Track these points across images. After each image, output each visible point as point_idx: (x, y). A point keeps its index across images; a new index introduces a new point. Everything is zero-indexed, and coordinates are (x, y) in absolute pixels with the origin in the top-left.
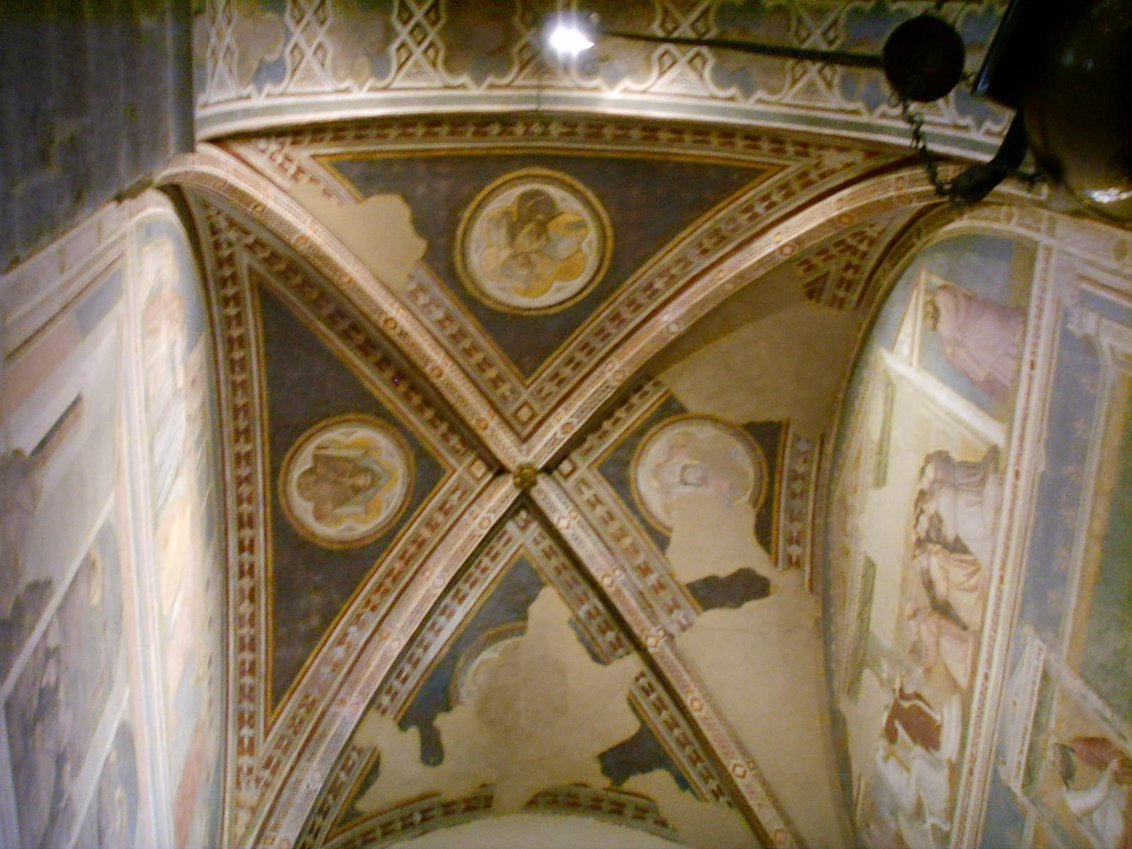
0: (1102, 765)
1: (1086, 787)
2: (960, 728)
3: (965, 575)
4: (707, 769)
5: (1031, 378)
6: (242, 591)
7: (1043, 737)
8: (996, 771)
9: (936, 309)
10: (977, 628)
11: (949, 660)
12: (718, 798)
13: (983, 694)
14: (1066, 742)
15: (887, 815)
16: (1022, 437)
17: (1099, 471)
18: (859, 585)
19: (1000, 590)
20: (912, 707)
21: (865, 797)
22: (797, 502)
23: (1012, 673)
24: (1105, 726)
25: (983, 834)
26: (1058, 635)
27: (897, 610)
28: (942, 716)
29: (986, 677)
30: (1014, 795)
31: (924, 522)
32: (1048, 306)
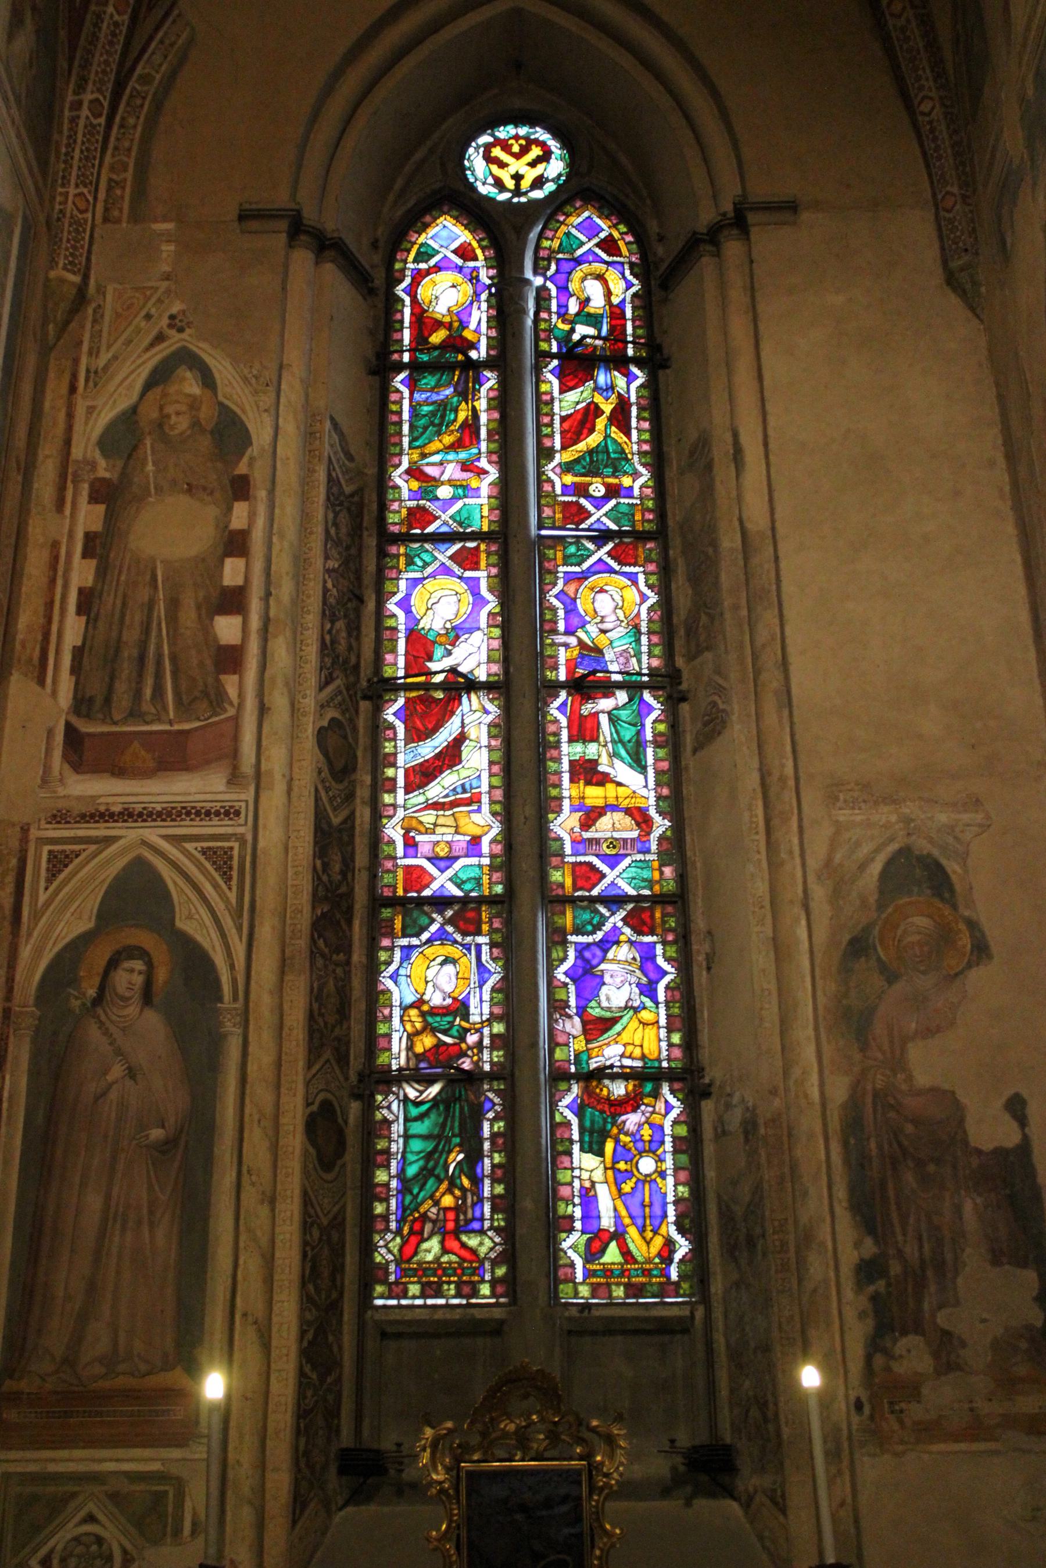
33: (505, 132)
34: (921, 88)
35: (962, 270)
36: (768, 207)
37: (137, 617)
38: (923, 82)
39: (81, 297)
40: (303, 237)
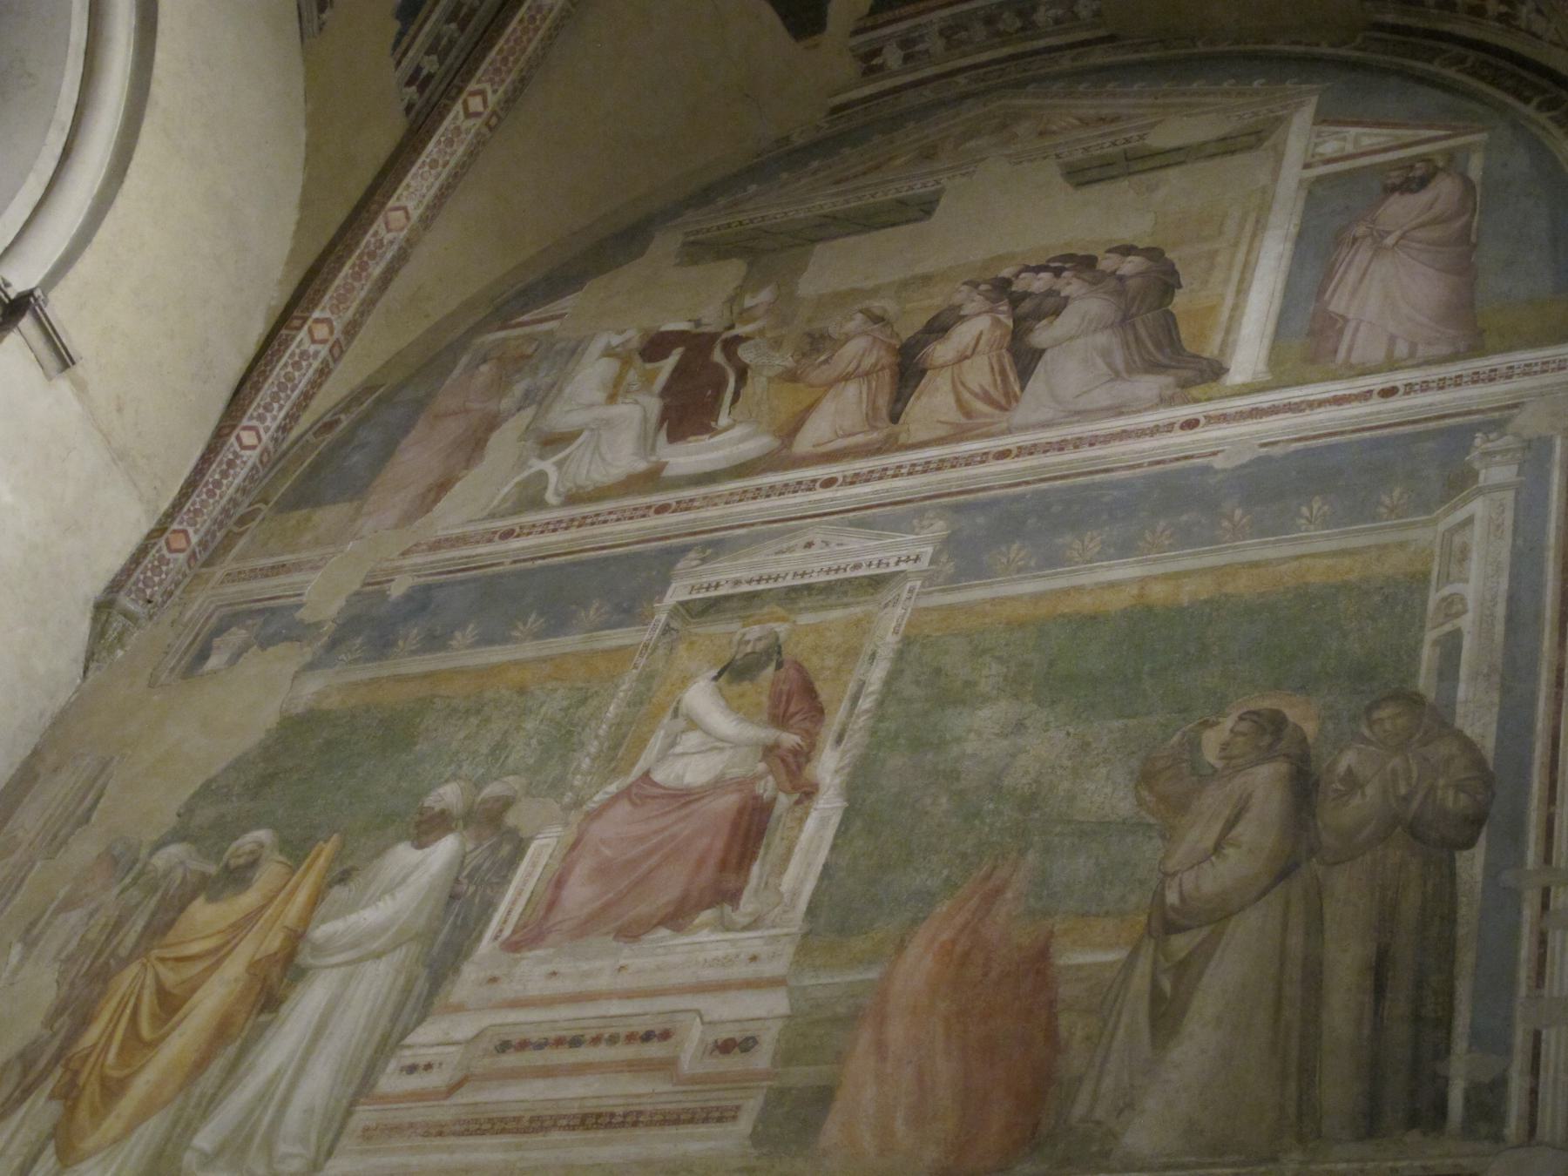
0: (780, 719)
1: (733, 706)
2: (723, 465)
3: (981, 386)
4: (452, 43)
5: (1366, 396)
7: (780, 611)
8: (685, 549)
9: (1423, 182)
10: (903, 439)
11: (828, 407)
12: (409, 83)
13: (798, 486)
14: (789, 652)
15: (518, 389)
16: (1256, 413)
17: (1255, 565)
18: (880, 198)
19: (984, 457)
20: (717, 366)
21: (530, 338)
22: (980, 32)
23: (861, 524)
24: (846, 704)
25: (574, 564)
26: (954, 582)
27: (869, 284)
28: (726, 429)
29: (829, 483)
30: (663, 593)
31: (1040, 283)
32: (1498, 390)
34: (261, 418)
35: (126, 614)
36: (50, 335)
38: (268, 415)
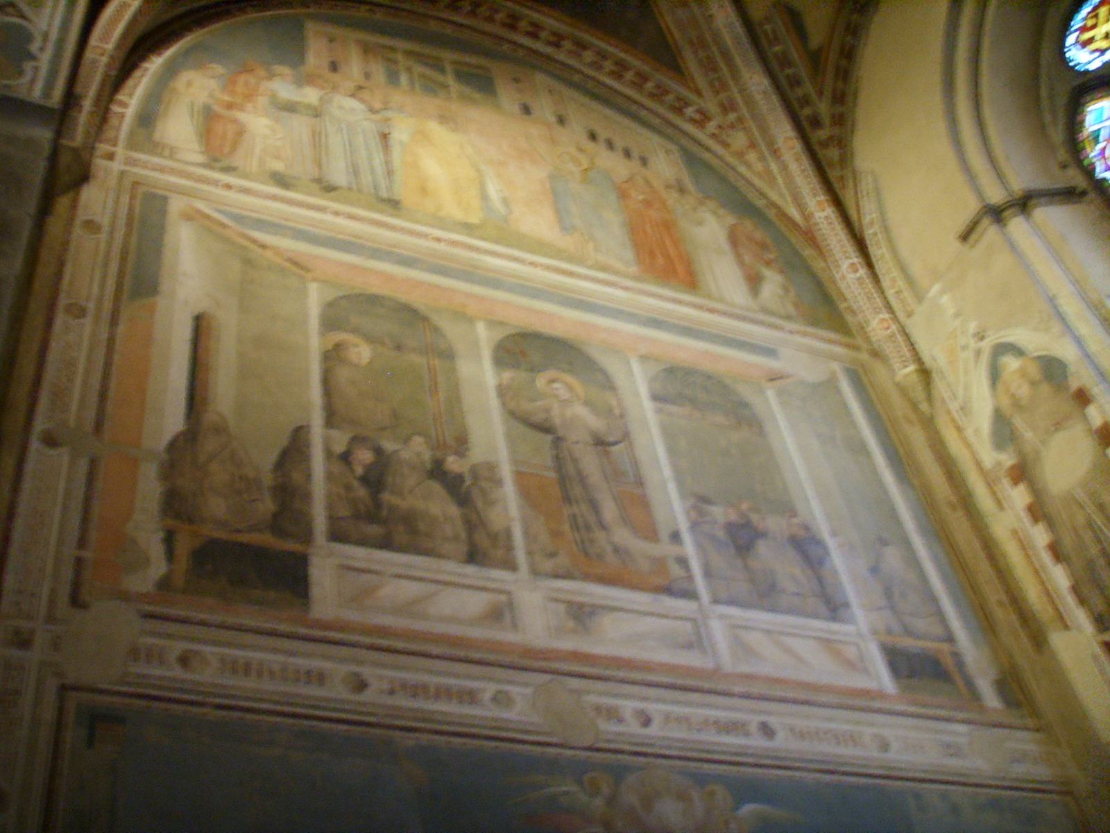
6: (570, 52)
33: (1077, 22)
37: (1088, 536)
39: (925, 373)
40: (1006, 214)
